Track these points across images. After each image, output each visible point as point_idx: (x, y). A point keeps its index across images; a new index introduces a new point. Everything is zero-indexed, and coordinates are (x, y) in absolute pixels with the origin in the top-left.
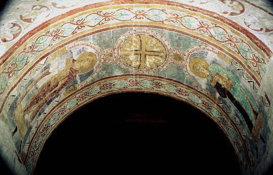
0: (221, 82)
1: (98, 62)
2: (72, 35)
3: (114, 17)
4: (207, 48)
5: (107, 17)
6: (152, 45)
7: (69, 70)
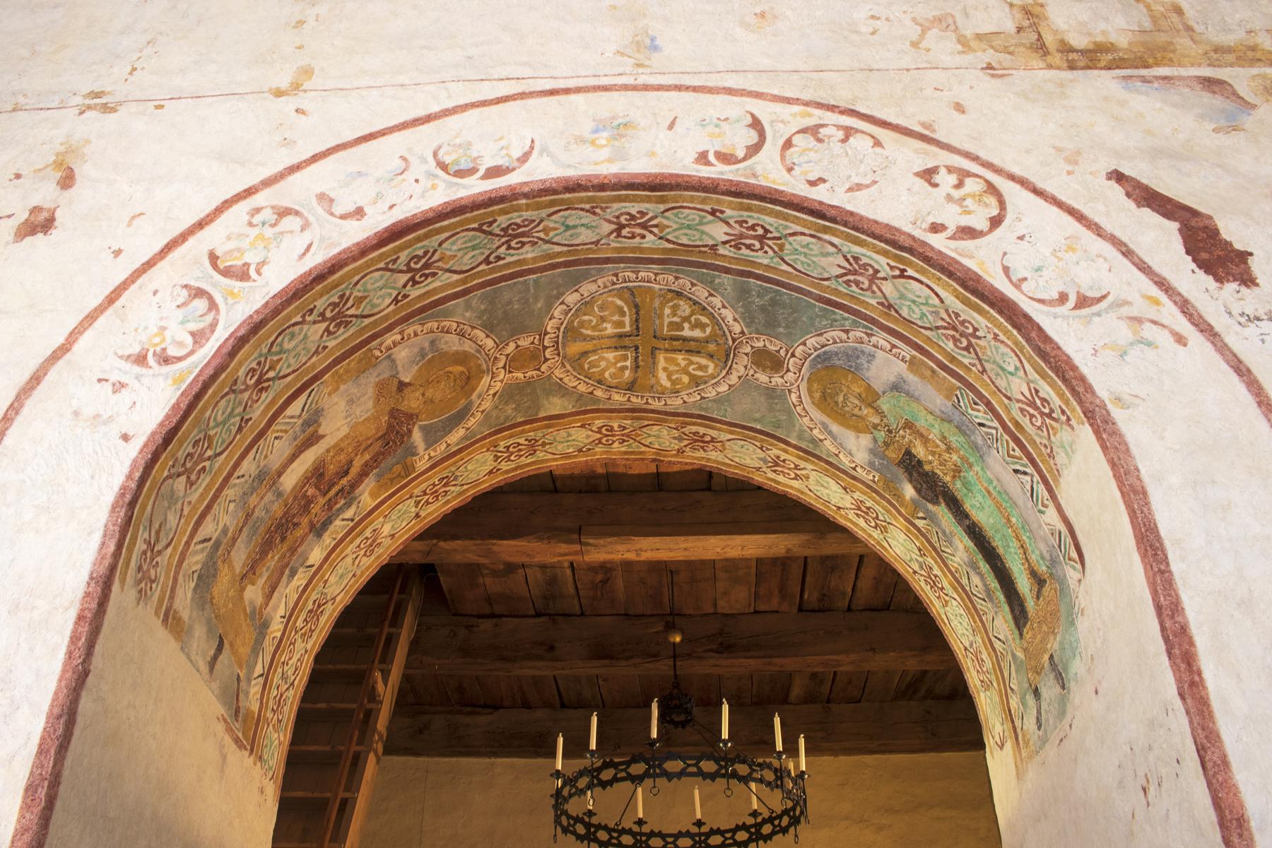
0: (920, 451)
3: (542, 235)
4: (874, 339)
5: (516, 236)
6: (676, 319)
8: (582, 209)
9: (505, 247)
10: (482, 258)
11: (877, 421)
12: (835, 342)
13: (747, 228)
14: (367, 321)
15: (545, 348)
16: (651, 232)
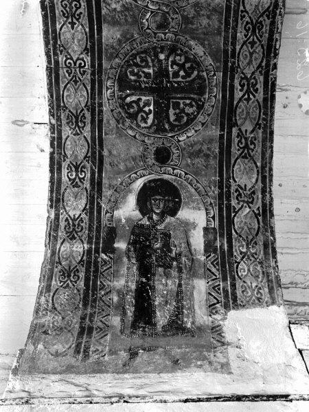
3: (251, 40)
6: (182, 106)
8: (262, 62)
9: (249, 21)
10: (248, 7)
11: (155, 217)
12: (196, 190)
13: (251, 141)
15: (165, 34)
16: (244, 95)
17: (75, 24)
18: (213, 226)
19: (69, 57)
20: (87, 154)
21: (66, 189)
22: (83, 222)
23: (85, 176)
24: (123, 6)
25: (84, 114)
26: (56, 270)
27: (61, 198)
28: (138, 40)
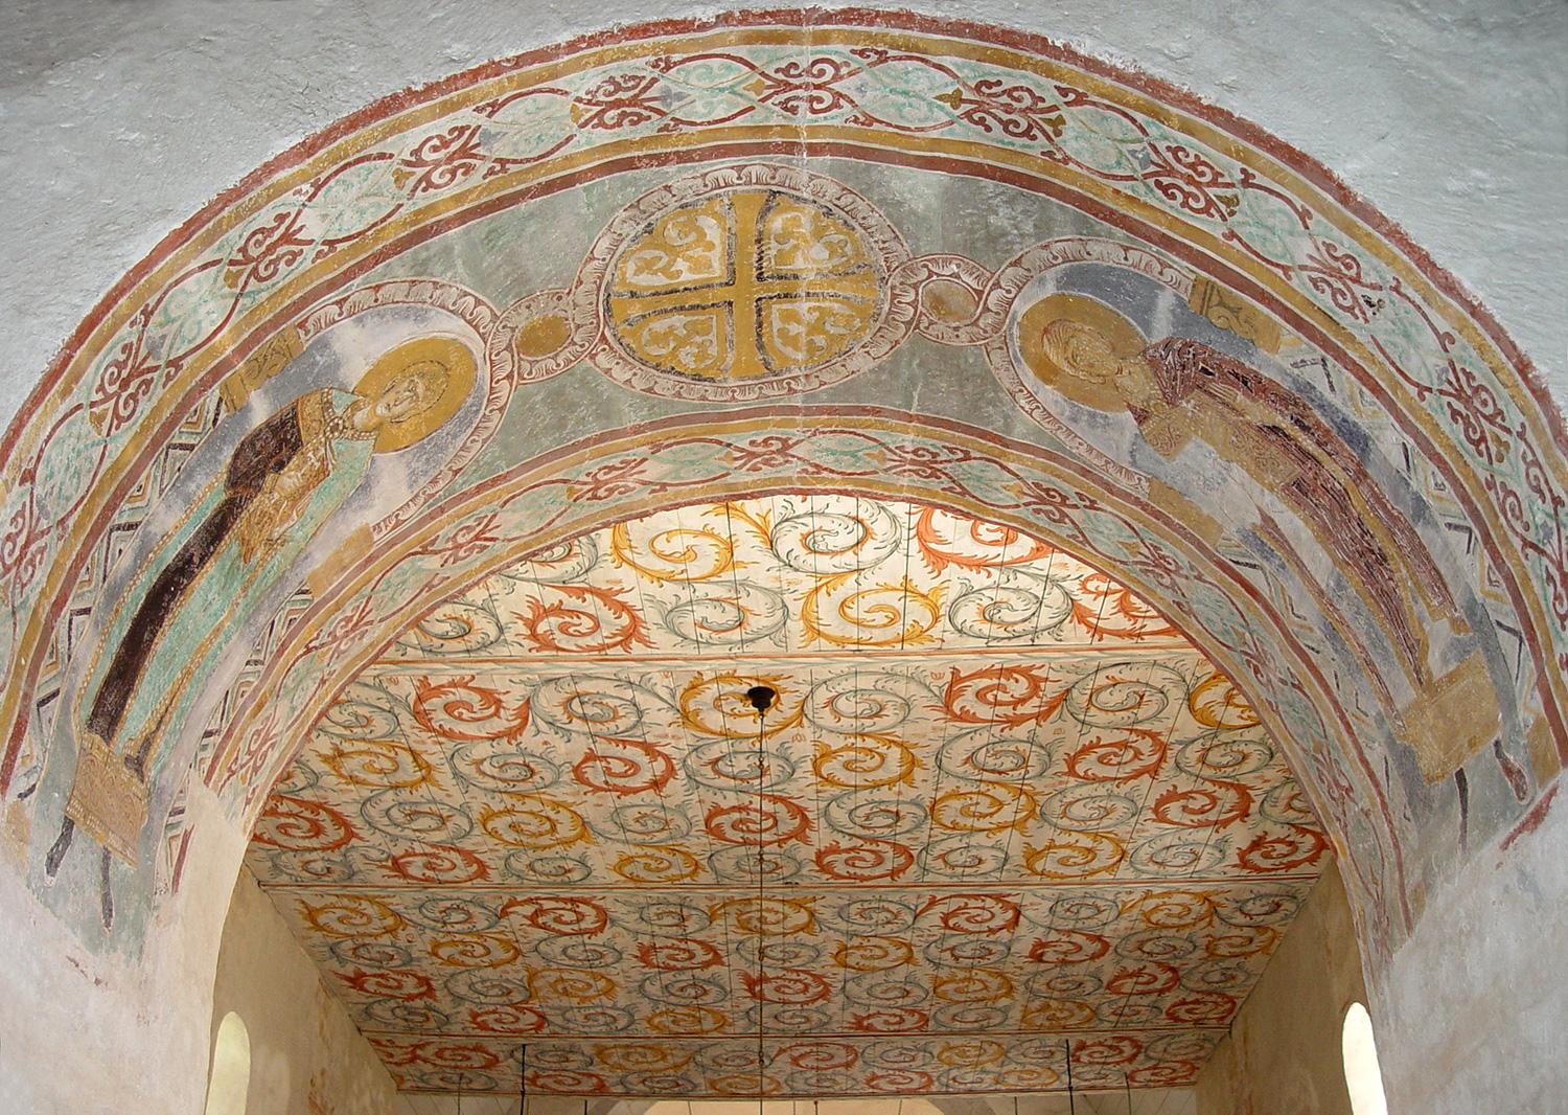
1: (1021, 307)
2: (1100, 504)
3: (889, 455)
5: (923, 464)
6: (698, 339)
7: (1187, 405)
11: (360, 418)
13: (618, 487)
14: (1135, 524)
16: (742, 450)
17: (955, 107)
18: (376, 538)
19: (844, 71)
20: (515, 162)
21: (382, 156)
22: (289, 263)
23: (438, 187)
24: (1004, 234)
25: (649, 117)
26: (125, 329)
27: (351, 159)
28: (894, 245)
